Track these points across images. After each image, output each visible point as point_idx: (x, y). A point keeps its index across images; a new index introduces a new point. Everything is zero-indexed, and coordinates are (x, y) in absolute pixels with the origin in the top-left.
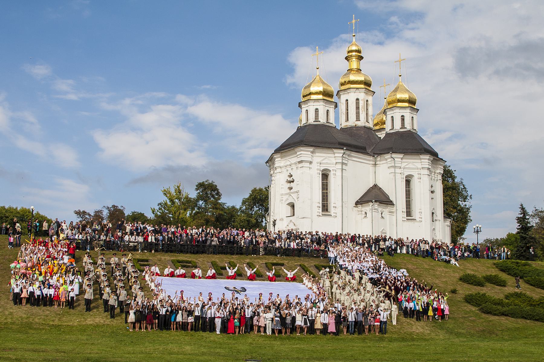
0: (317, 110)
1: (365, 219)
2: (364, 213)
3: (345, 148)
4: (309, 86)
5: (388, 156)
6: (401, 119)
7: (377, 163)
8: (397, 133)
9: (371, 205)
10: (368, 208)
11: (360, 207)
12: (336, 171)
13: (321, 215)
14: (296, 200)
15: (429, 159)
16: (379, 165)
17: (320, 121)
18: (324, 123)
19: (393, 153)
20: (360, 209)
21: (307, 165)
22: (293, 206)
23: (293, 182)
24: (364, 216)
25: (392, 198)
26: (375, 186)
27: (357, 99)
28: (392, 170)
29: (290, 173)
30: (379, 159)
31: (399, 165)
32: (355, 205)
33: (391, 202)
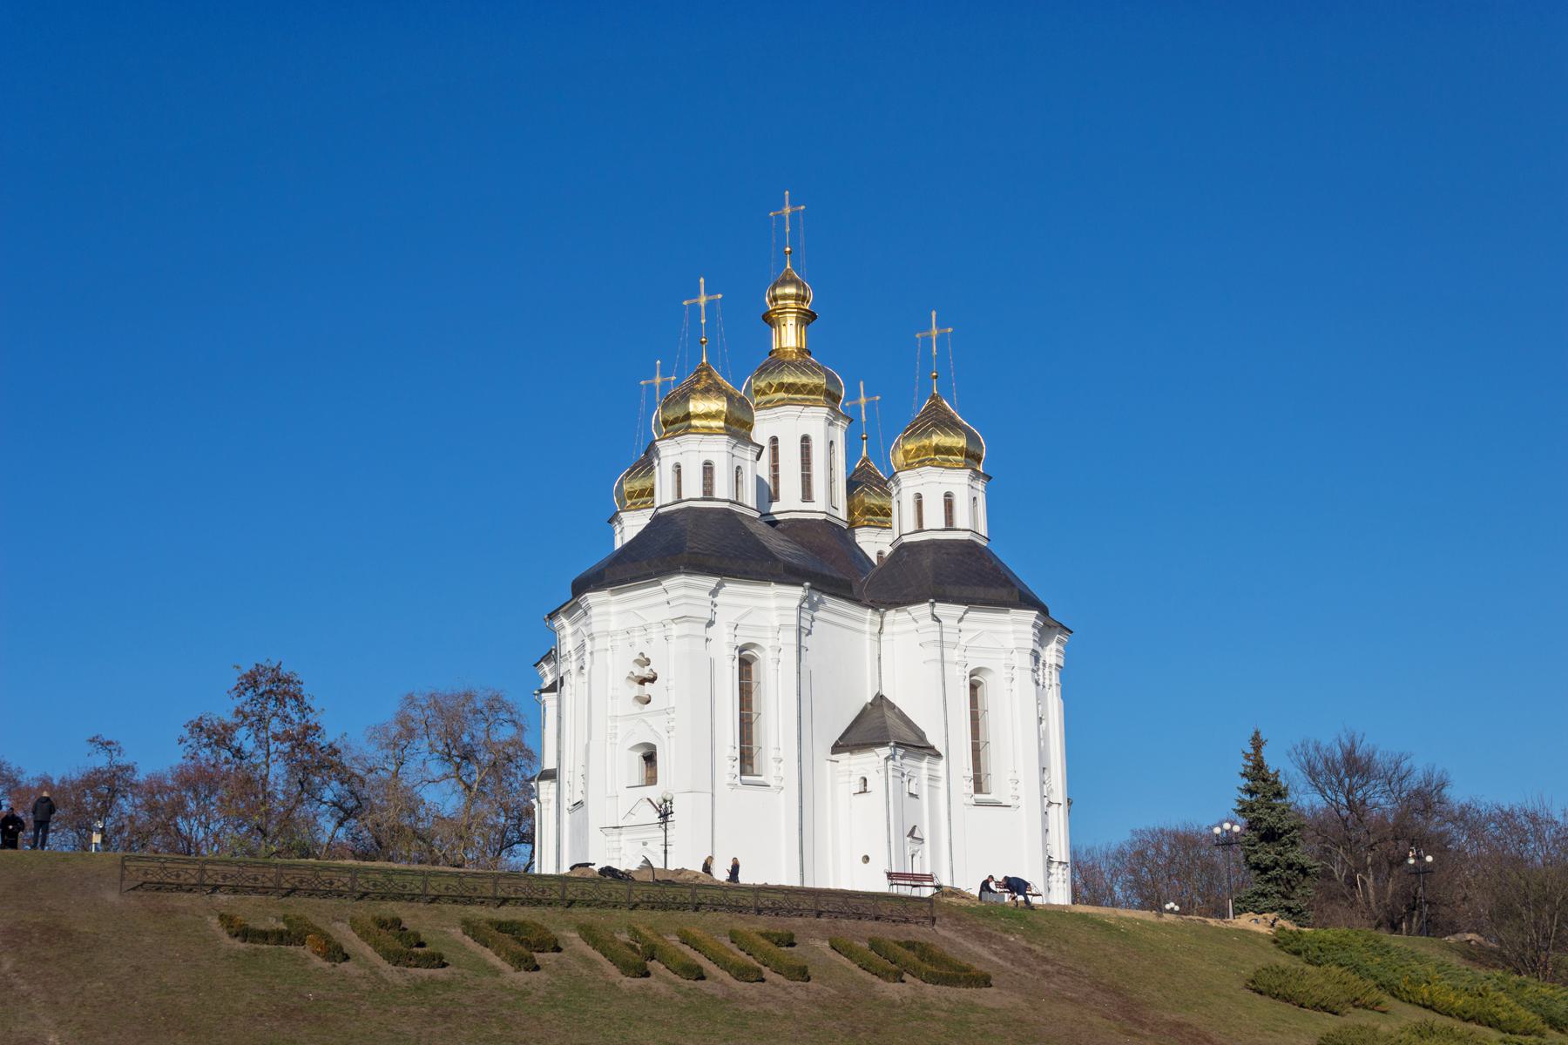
0: (708, 469)
3: (807, 584)
4: (685, 398)
5: (923, 610)
6: (945, 501)
10: (872, 762)
13: (739, 784)
14: (664, 736)
15: (1035, 626)
19: (936, 601)
22: (650, 758)
23: (652, 680)
25: (933, 739)
26: (880, 699)
27: (805, 439)
29: (642, 654)
31: (954, 638)
33: (932, 748)
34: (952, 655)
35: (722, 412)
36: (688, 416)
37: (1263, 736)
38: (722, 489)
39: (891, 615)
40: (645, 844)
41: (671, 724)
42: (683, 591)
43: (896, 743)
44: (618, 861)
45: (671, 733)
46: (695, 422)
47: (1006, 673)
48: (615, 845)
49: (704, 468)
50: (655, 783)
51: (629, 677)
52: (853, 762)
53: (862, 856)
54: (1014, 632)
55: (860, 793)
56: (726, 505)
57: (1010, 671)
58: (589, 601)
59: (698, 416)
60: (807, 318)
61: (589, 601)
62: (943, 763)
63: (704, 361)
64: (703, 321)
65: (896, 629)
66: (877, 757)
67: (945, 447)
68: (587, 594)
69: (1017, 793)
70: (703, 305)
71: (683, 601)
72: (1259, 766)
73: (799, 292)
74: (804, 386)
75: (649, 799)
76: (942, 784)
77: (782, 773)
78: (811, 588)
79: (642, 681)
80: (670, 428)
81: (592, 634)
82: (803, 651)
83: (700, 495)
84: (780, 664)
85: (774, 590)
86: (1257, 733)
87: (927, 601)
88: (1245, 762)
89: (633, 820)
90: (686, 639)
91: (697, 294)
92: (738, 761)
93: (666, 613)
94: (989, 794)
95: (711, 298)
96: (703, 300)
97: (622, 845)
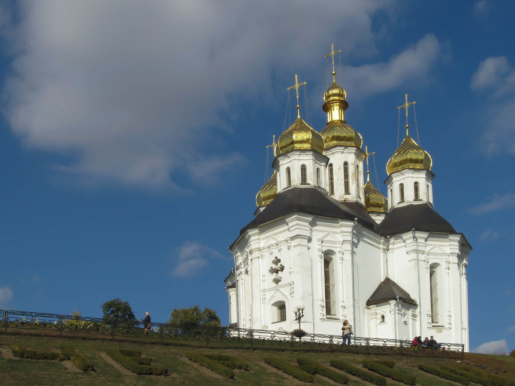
1: (383, 325)
2: (379, 316)
5: (410, 235)
7: (391, 247)
8: (410, 207)
9: (392, 304)
11: (373, 308)
12: (343, 254)
13: (326, 319)
14: (289, 296)
16: (392, 251)
17: (309, 184)
18: (315, 186)
20: (374, 311)
24: (380, 320)
25: (413, 296)
28: (414, 256)
29: (276, 258)
30: (392, 240)
32: (365, 306)
33: (413, 301)
38: (311, 181)
41: (292, 290)
45: (292, 295)
54: (450, 245)
57: (448, 264)
69: (450, 322)
73: (340, 93)
77: (345, 313)
81: (251, 250)
82: (354, 254)
84: (343, 261)
92: (325, 308)
94: (438, 323)
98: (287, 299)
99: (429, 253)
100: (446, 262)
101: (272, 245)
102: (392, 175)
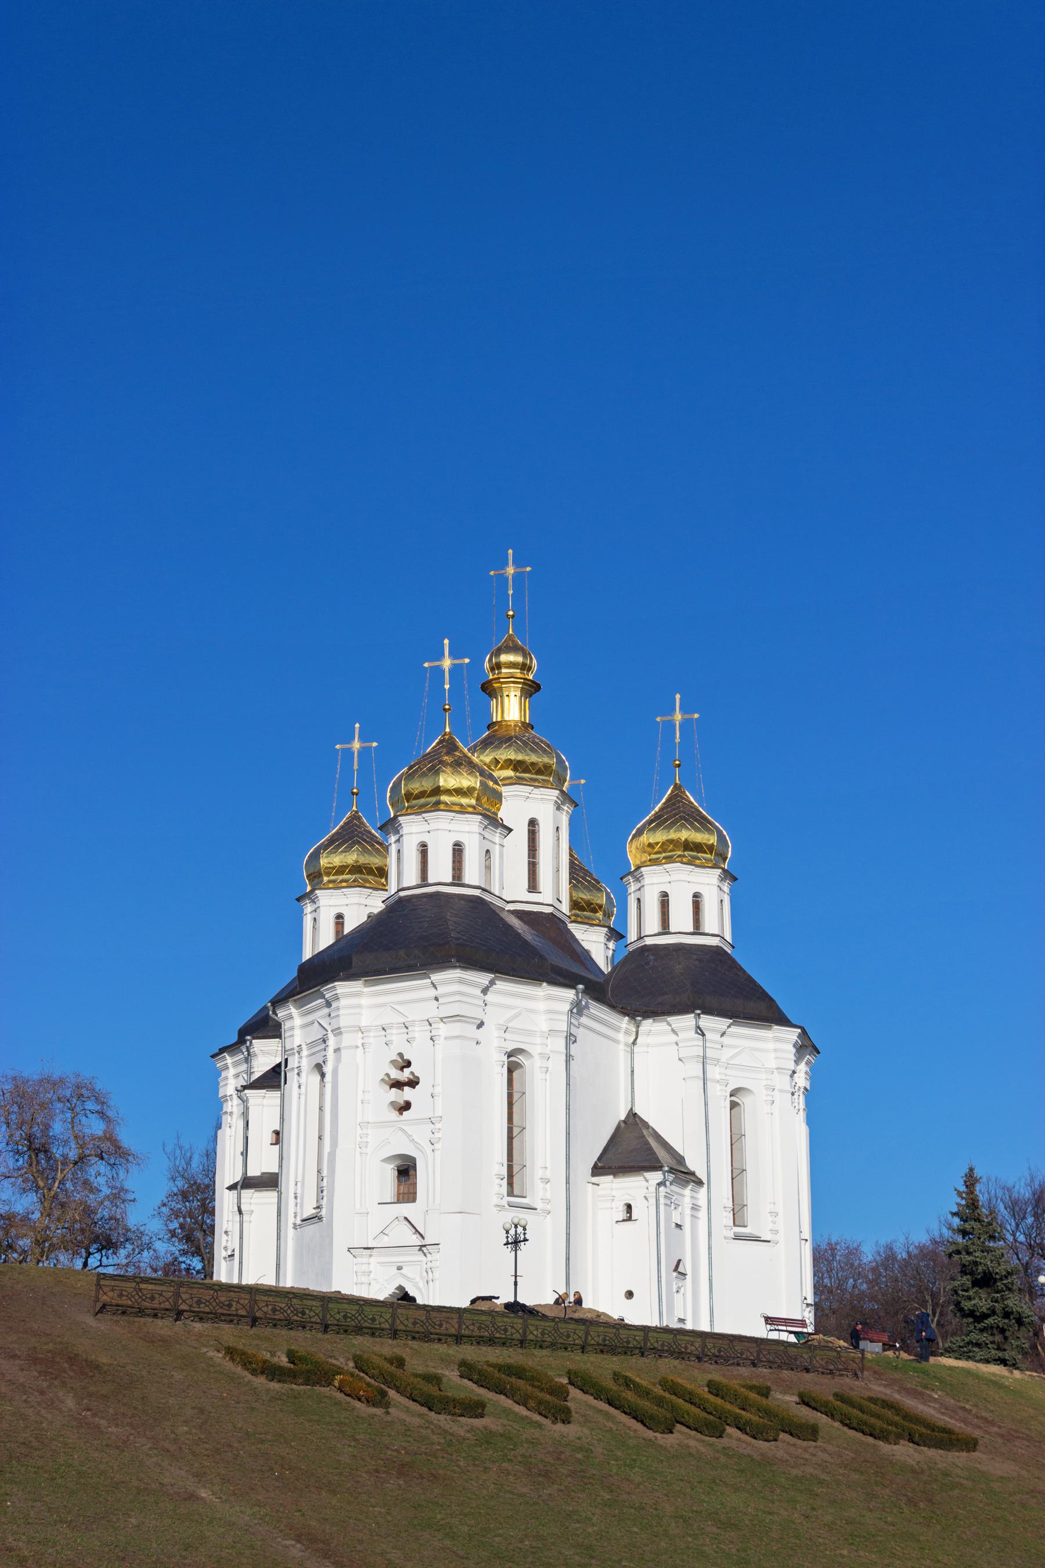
0: (458, 850)
3: (581, 987)
11: (606, 1180)
14: (428, 1148)
19: (703, 1013)
21: (471, 1030)
22: (406, 1170)
24: (622, 1215)
25: (694, 1163)
26: (632, 1115)
27: (533, 823)
29: (401, 1055)
33: (693, 1174)
34: (713, 1072)
35: (474, 789)
36: (437, 791)
37: (977, 1173)
38: (472, 874)
39: (647, 1025)
40: (399, 1268)
42: (456, 987)
43: (671, 1168)
44: (367, 1286)
45: (437, 1146)
46: (444, 798)
47: (767, 1095)
48: (364, 1268)
49: (454, 850)
50: (414, 1200)
51: (383, 1080)
52: (614, 1186)
53: (626, 1290)
54: (775, 1050)
55: (624, 1220)
56: (477, 893)
58: (338, 992)
59: (448, 792)
60: (531, 689)
61: (338, 992)
62: (704, 1190)
63: (448, 730)
64: (447, 687)
65: (650, 1040)
66: (645, 1183)
67: (694, 843)
68: (336, 983)
70: (447, 670)
71: (457, 998)
72: (973, 1204)
73: (525, 662)
74: (533, 764)
75: (406, 1218)
76: (703, 1214)
77: (548, 1195)
78: (584, 992)
79: (398, 1085)
80: (414, 802)
83: (449, 880)
85: (545, 990)
86: (971, 1170)
87: (693, 1012)
88: (959, 1200)
89: (385, 1241)
90: (458, 1041)
91: (440, 656)
92: (505, 1180)
93: (431, 1010)
95: (457, 662)
96: (447, 663)
97: (372, 1267)
98: (421, 1151)
99: (729, 1066)
100: (767, 1087)
101: (391, 1026)
102: (643, 869)
